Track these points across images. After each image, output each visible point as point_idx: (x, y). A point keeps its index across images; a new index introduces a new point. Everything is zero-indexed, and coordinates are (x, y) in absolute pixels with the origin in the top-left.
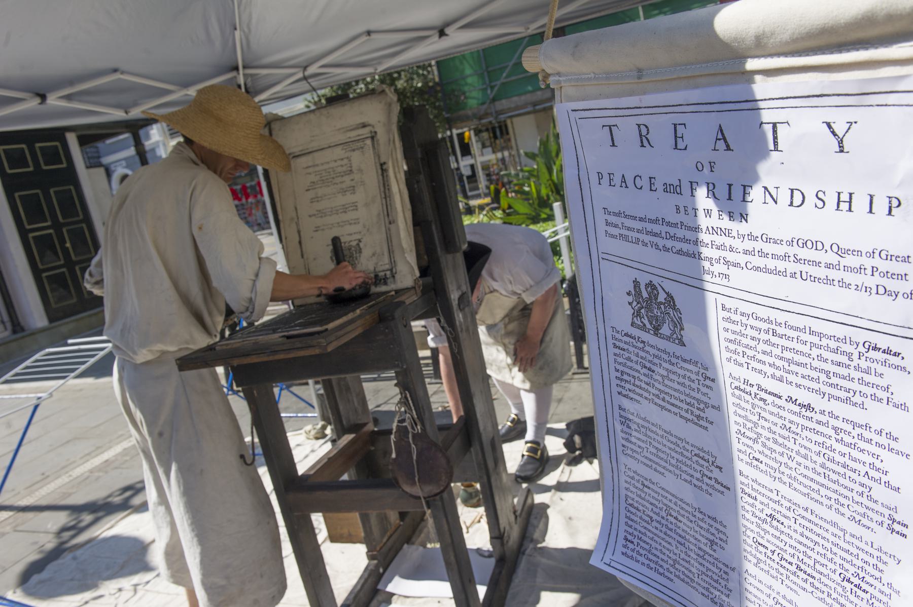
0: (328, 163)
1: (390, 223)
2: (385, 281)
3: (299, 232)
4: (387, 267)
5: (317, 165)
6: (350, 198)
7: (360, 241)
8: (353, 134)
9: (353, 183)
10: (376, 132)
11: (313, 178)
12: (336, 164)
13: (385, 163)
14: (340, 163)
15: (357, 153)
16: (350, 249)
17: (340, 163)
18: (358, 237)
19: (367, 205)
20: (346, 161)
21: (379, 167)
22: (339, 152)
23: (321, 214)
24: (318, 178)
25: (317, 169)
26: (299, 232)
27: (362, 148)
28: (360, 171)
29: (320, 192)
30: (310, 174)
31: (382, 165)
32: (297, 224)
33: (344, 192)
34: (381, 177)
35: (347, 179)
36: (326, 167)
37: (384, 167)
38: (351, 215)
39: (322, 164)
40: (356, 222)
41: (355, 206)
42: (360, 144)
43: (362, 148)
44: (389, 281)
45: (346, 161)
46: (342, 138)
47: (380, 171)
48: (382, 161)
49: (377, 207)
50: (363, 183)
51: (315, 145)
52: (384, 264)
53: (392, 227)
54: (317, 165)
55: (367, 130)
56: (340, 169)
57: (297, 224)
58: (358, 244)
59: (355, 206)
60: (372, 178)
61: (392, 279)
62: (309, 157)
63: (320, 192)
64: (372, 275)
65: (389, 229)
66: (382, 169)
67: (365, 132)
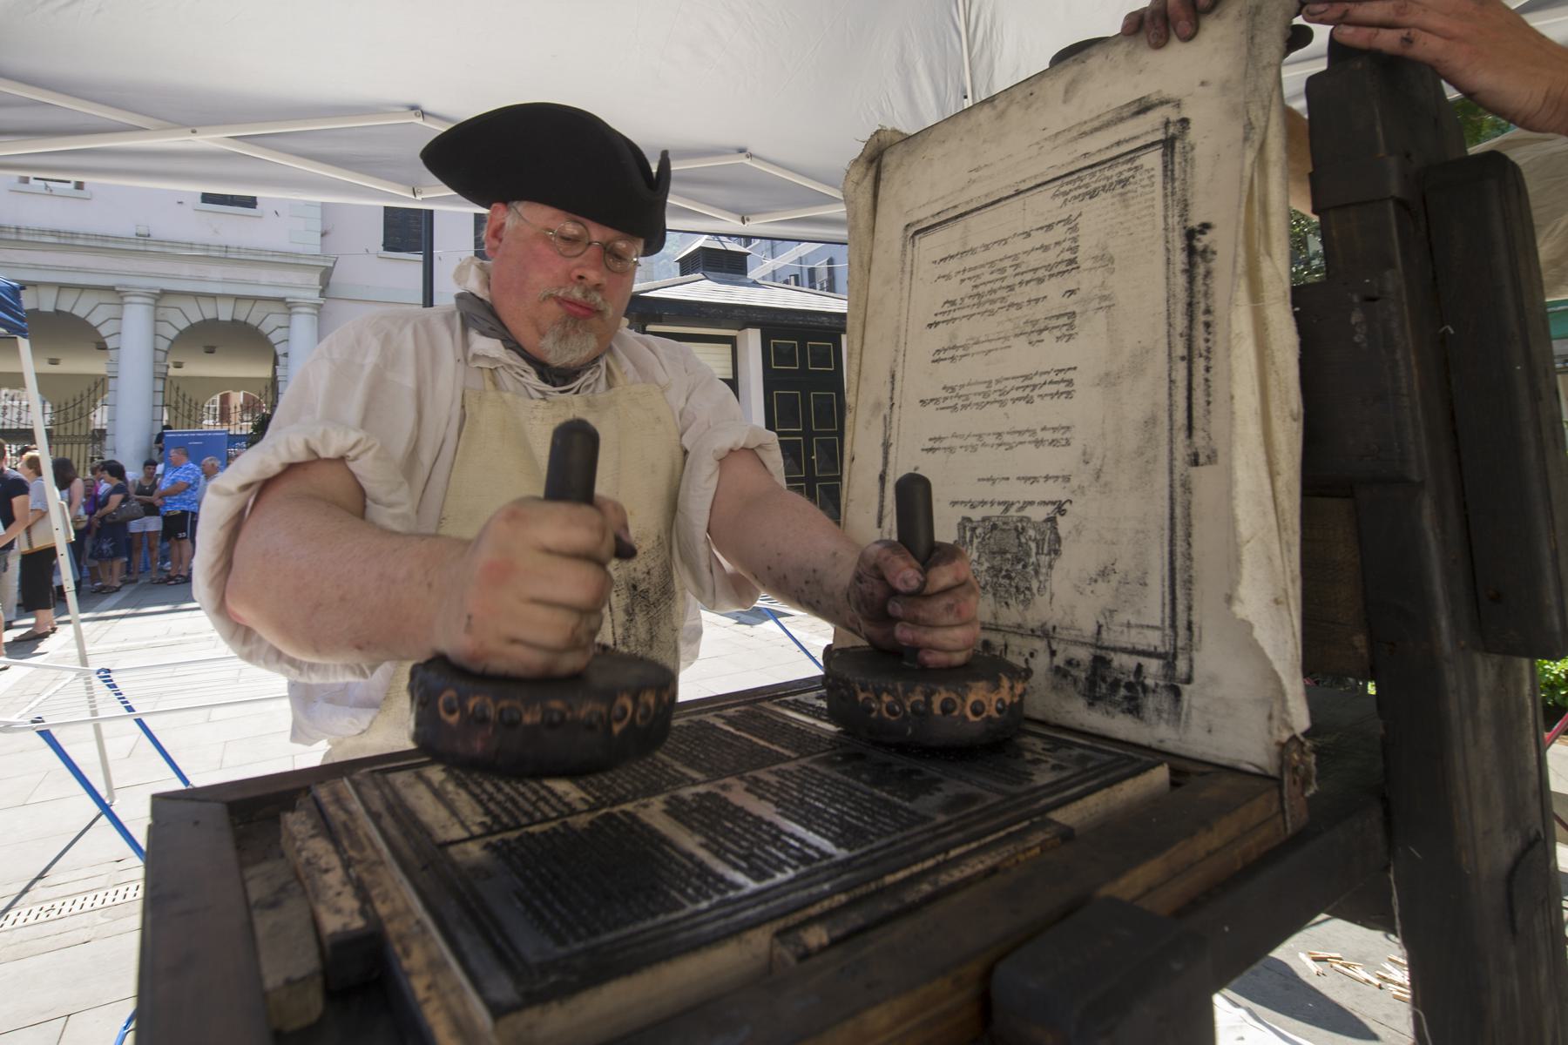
0: (1005, 241)
1: (1195, 462)
2: (1132, 696)
3: (886, 446)
4: (1153, 639)
5: (973, 251)
6: (1051, 353)
7: (1061, 510)
8: (1097, 144)
9: (1070, 304)
10: (1185, 122)
11: (954, 289)
12: (1028, 244)
13: (1206, 227)
14: (1040, 238)
15: (1104, 199)
16: (1020, 532)
17: (1040, 238)
18: (1056, 492)
19: (1108, 380)
20: (1060, 232)
21: (1178, 243)
22: (1044, 205)
23: (953, 398)
24: (967, 288)
25: (970, 261)
26: (886, 446)
27: (1124, 182)
28: (1106, 260)
29: (965, 330)
30: (947, 277)
31: (1190, 235)
32: (887, 422)
33: (1035, 332)
34: (1181, 280)
35: (1053, 290)
36: (996, 253)
37: (1202, 241)
38: (1046, 413)
39: (986, 247)
40: (1060, 437)
41: (1064, 384)
42: (1112, 173)
43: (1124, 182)
44: (1150, 702)
45: (1060, 232)
46: (1061, 159)
47: (1180, 258)
48: (1194, 223)
49: (1148, 393)
50: (1106, 302)
51: (978, 193)
52: (1142, 623)
53: (1203, 478)
54: (973, 251)
55: (1155, 117)
56: (1036, 259)
57: (887, 422)
58: (1051, 520)
59: (1064, 384)
60: (1146, 286)
61: (1165, 701)
62: (956, 229)
63: (965, 330)
64: (1084, 655)
65: (1187, 487)
66: (1191, 251)
67: (1149, 126)
